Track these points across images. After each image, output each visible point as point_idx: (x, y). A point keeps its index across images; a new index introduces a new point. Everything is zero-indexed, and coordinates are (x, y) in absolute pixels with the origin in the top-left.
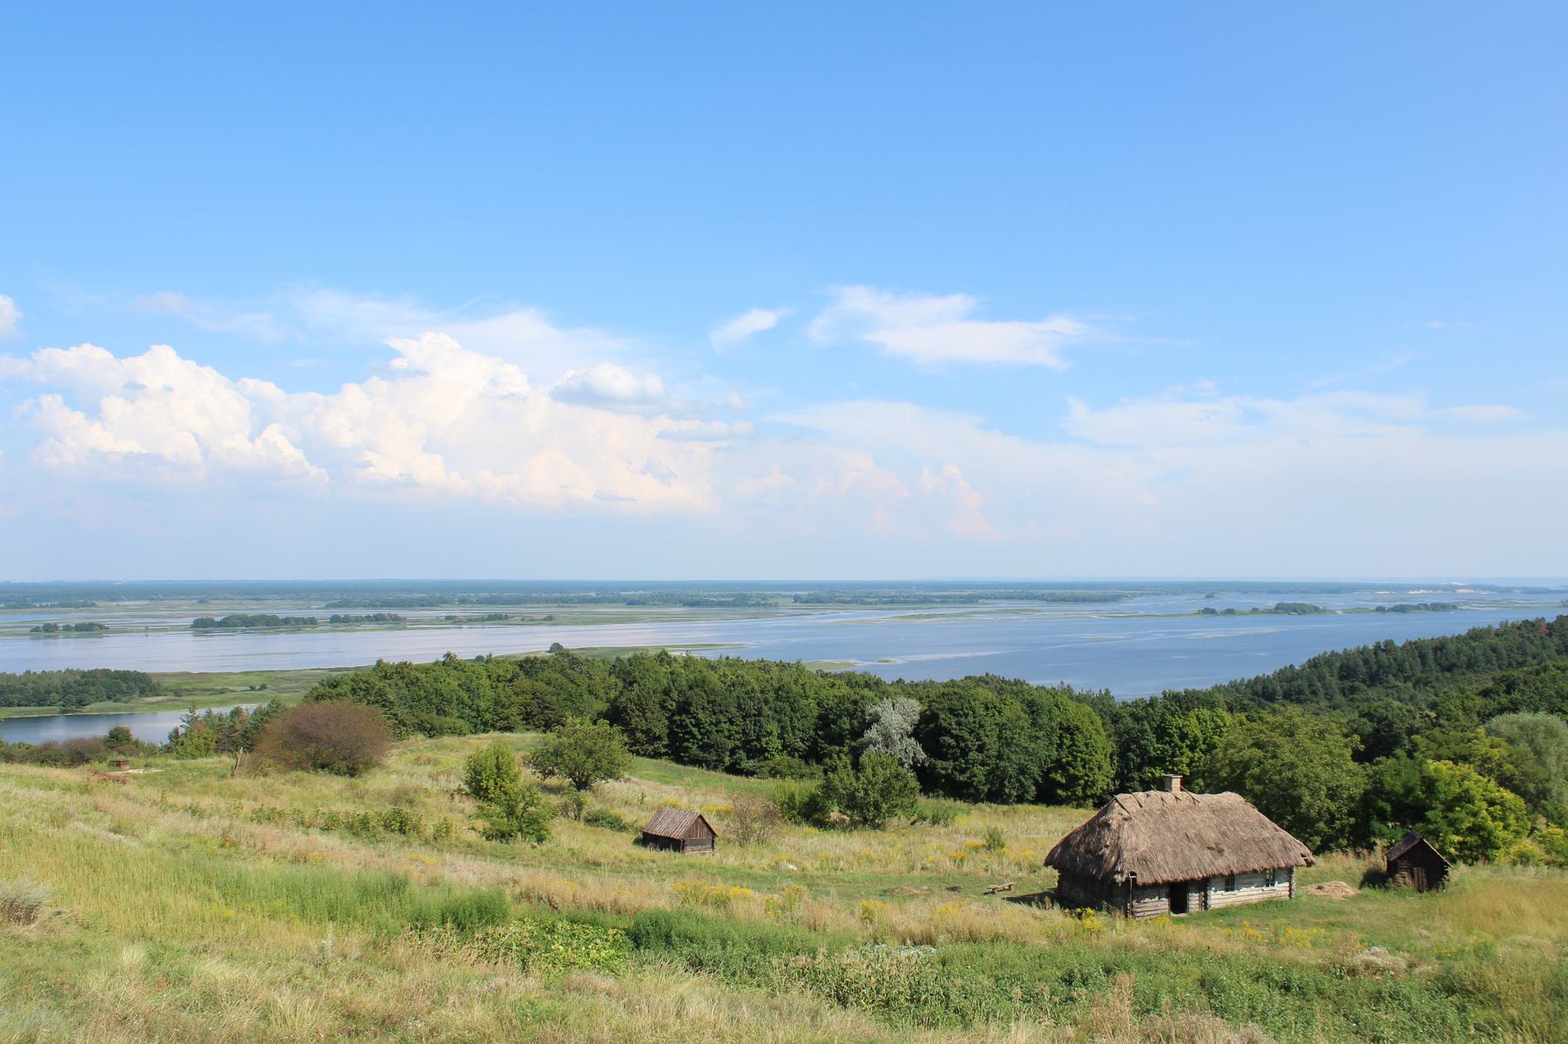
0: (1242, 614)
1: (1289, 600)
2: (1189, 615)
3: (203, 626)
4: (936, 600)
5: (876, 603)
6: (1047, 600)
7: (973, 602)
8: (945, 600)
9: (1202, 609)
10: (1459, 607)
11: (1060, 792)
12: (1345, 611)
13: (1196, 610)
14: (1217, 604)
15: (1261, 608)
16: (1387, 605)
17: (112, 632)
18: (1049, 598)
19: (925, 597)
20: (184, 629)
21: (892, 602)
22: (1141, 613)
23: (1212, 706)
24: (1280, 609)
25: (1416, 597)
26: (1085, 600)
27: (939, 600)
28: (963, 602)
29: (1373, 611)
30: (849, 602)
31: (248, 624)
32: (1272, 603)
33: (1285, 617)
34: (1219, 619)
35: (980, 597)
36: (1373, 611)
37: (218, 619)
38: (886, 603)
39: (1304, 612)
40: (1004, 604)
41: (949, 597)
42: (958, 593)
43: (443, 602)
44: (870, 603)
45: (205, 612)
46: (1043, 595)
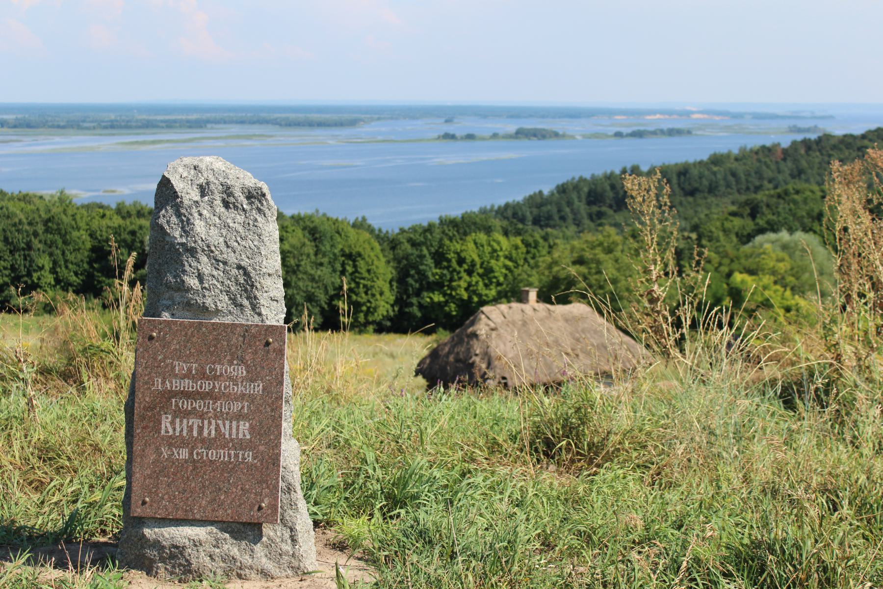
0: (483, 139)
2: (428, 140)
4: (161, 124)
5: (94, 128)
6: (281, 125)
7: (201, 127)
8: (170, 125)
9: (442, 133)
10: (694, 133)
12: (584, 136)
13: (436, 135)
14: (459, 128)
15: (501, 132)
16: (625, 130)
18: (283, 123)
19: (148, 121)
21: (112, 127)
22: (380, 138)
24: (520, 134)
25: (652, 122)
26: (321, 124)
27: (164, 125)
28: (190, 127)
29: (611, 136)
30: (63, 127)
33: (525, 142)
34: (460, 144)
35: (208, 121)
36: (611, 136)
38: (105, 128)
39: (544, 137)
40: (235, 129)
41: (175, 121)
42: (184, 117)
46: (276, 119)
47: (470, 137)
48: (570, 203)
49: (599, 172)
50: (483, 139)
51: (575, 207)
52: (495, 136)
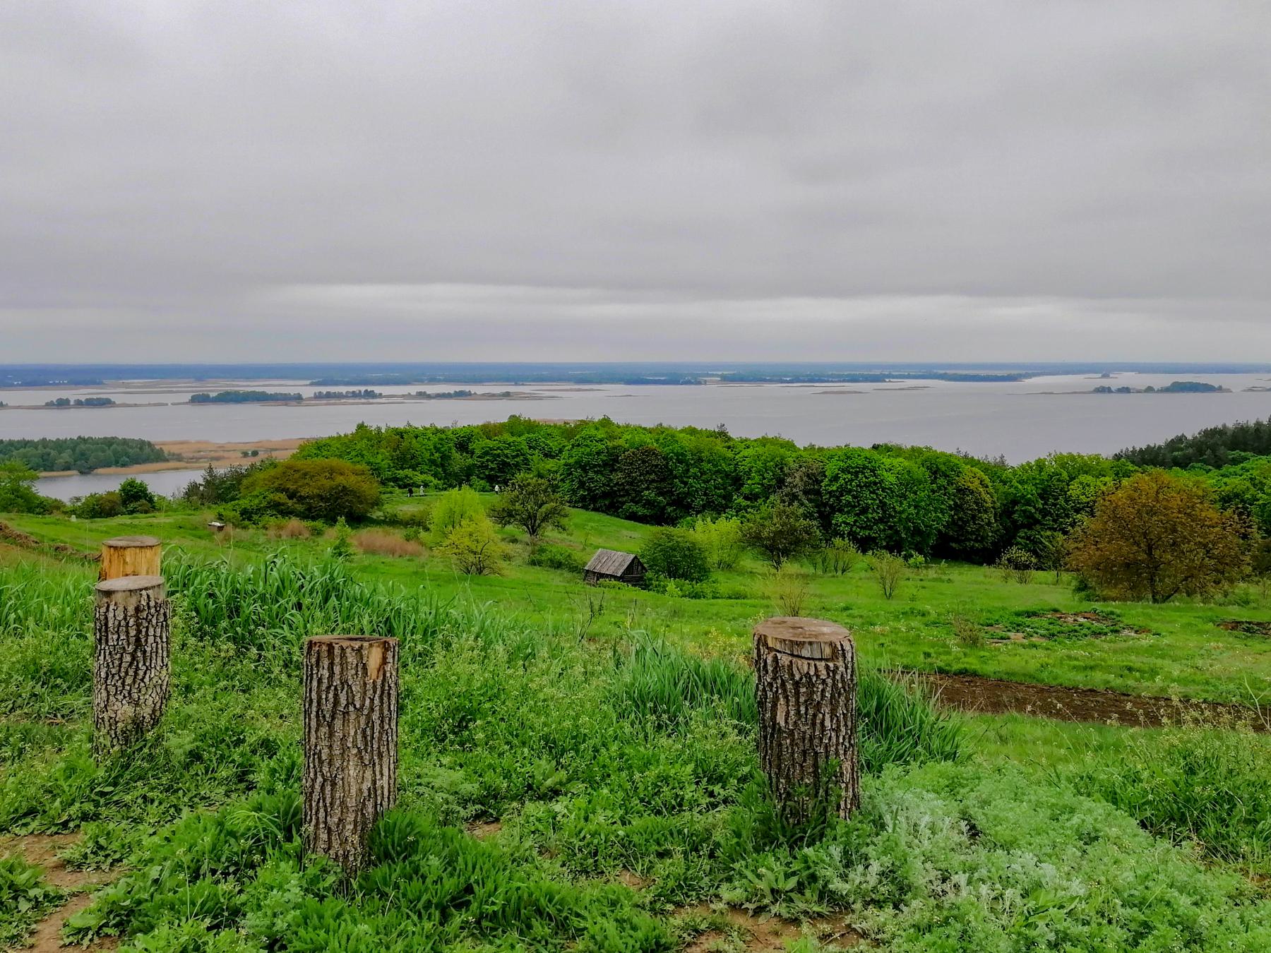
11: (954, 545)
20: (187, 403)
37: (212, 395)
45: (201, 388)
47: (1125, 390)
50: (1139, 392)
52: (1149, 389)
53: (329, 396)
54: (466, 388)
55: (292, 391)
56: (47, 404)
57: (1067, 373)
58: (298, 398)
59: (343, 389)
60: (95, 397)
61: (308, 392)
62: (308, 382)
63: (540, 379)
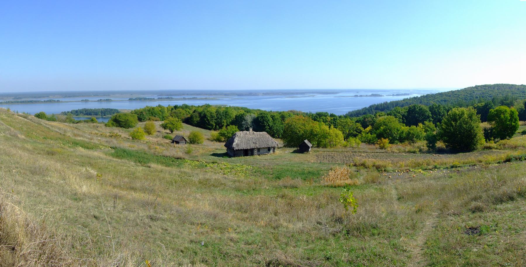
1: (374, 93)
3: (131, 100)
8: (297, 93)
10: (410, 94)
14: (359, 94)
15: (368, 95)
17: (113, 101)
21: (285, 94)
23: (326, 116)
31: (140, 99)
32: (370, 94)
37: (134, 98)
43: (183, 94)
44: (280, 94)
45: (131, 97)
48: (371, 110)
49: (379, 103)
51: (372, 111)
53: (161, 98)
54: (196, 97)
55: (152, 97)
56: (98, 100)
57: (381, 92)
58: (154, 99)
59: (165, 97)
60: (108, 99)
61: (156, 98)
62: (157, 95)
63: (215, 94)
